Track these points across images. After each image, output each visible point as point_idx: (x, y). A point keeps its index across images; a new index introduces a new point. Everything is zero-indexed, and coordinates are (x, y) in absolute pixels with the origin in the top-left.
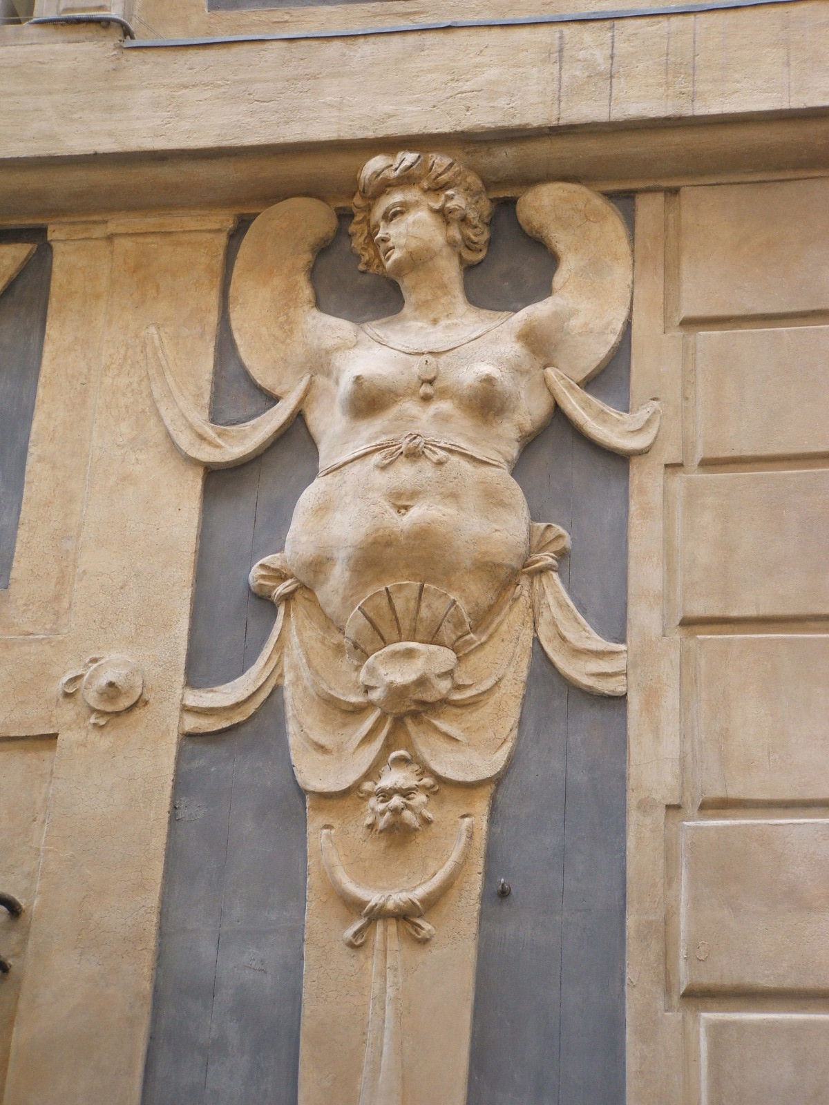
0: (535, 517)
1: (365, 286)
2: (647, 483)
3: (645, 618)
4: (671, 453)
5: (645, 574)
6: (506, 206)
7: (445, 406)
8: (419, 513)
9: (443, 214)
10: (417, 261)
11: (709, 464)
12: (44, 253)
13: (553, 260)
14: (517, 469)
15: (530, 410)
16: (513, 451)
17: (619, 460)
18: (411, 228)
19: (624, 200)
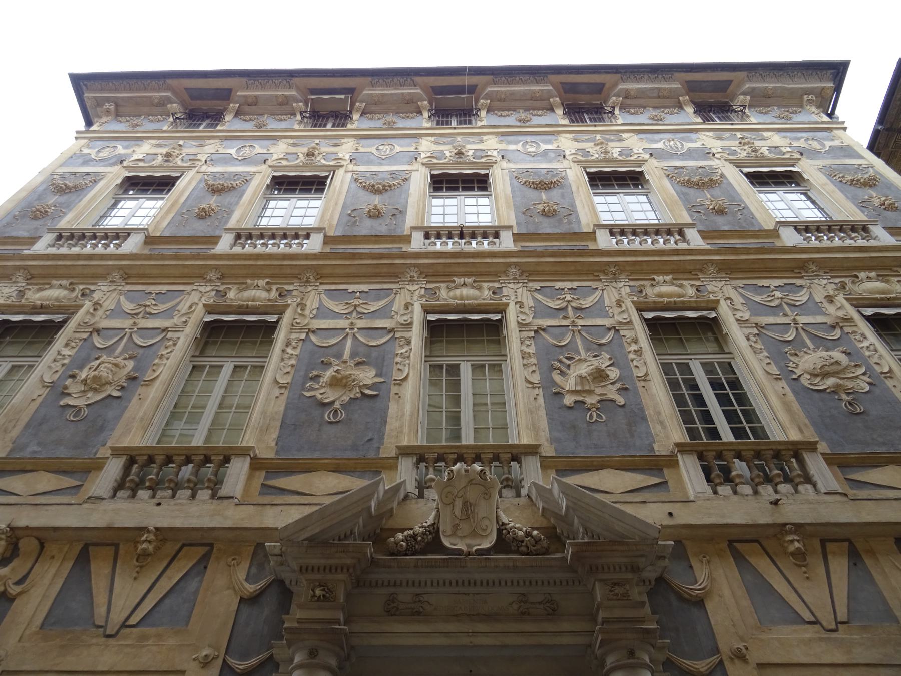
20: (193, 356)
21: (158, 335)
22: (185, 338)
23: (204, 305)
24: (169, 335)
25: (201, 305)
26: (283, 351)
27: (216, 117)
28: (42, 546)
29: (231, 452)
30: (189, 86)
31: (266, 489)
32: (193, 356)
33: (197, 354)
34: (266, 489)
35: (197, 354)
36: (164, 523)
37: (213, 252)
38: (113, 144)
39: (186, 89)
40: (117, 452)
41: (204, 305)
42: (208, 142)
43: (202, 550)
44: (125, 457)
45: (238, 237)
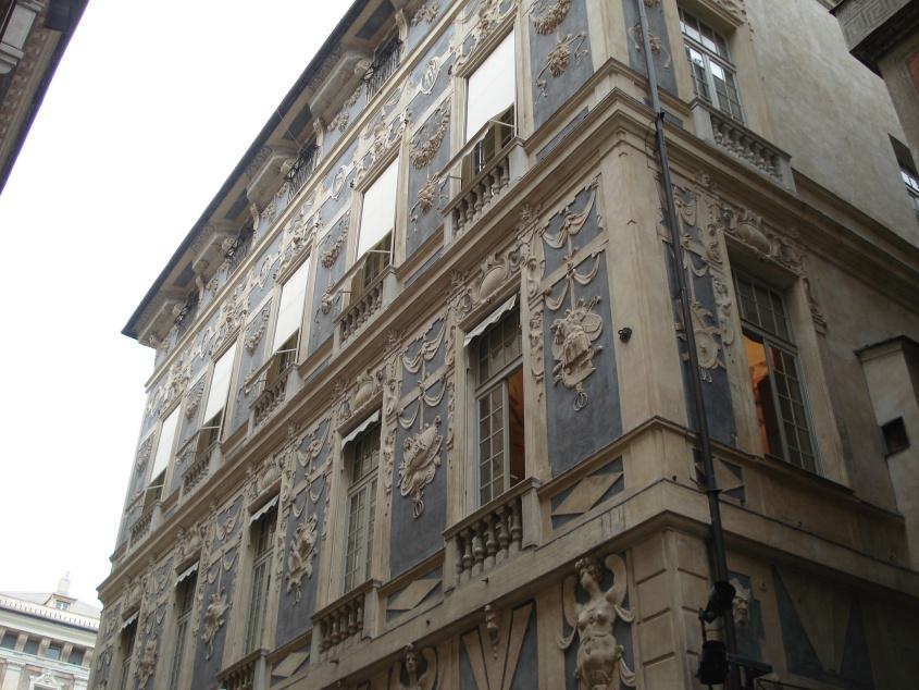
0: (618, 643)
1: (584, 596)
2: (634, 628)
3: (637, 665)
4: (637, 620)
5: (636, 654)
6: (603, 564)
7: (595, 624)
8: (593, 653)
9: (590, 573)
10: (589, 585)
11: (645, 620)
12: (535, 604)
13: (613, 575)
14: (614, 633)
15: (612, 618)
16: (611, 629)
17: (629, 625)
18: (586, 578)
19: (623, 555)
20: (476, 391)
21: (442, 387)
22: (459, 378)
23: (461, 326)
24: (449, 382)
25: (457, 328)
26: (531, 337)
27: (396, 44)
28: (435, 648)
29: (519, 492)
30: (356, 32)
31: (557, 520)
32: (476, 391)
33: (479, 385)
34: (557, 520)
35: (479, 385)
36: (497, 592)
37: (444, 253)
38: (336, 169)
39: (357, 35)
40: (448, 535)
41: (461, 326)
42: (401, 87)
43: (527, 609)
44: (455, 538)
45: (457, 215)
